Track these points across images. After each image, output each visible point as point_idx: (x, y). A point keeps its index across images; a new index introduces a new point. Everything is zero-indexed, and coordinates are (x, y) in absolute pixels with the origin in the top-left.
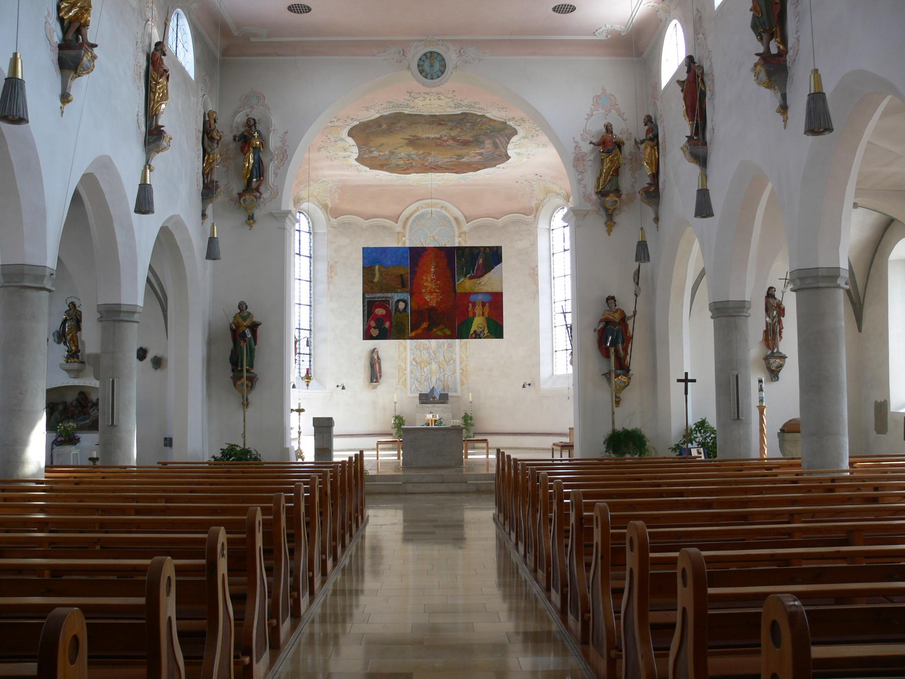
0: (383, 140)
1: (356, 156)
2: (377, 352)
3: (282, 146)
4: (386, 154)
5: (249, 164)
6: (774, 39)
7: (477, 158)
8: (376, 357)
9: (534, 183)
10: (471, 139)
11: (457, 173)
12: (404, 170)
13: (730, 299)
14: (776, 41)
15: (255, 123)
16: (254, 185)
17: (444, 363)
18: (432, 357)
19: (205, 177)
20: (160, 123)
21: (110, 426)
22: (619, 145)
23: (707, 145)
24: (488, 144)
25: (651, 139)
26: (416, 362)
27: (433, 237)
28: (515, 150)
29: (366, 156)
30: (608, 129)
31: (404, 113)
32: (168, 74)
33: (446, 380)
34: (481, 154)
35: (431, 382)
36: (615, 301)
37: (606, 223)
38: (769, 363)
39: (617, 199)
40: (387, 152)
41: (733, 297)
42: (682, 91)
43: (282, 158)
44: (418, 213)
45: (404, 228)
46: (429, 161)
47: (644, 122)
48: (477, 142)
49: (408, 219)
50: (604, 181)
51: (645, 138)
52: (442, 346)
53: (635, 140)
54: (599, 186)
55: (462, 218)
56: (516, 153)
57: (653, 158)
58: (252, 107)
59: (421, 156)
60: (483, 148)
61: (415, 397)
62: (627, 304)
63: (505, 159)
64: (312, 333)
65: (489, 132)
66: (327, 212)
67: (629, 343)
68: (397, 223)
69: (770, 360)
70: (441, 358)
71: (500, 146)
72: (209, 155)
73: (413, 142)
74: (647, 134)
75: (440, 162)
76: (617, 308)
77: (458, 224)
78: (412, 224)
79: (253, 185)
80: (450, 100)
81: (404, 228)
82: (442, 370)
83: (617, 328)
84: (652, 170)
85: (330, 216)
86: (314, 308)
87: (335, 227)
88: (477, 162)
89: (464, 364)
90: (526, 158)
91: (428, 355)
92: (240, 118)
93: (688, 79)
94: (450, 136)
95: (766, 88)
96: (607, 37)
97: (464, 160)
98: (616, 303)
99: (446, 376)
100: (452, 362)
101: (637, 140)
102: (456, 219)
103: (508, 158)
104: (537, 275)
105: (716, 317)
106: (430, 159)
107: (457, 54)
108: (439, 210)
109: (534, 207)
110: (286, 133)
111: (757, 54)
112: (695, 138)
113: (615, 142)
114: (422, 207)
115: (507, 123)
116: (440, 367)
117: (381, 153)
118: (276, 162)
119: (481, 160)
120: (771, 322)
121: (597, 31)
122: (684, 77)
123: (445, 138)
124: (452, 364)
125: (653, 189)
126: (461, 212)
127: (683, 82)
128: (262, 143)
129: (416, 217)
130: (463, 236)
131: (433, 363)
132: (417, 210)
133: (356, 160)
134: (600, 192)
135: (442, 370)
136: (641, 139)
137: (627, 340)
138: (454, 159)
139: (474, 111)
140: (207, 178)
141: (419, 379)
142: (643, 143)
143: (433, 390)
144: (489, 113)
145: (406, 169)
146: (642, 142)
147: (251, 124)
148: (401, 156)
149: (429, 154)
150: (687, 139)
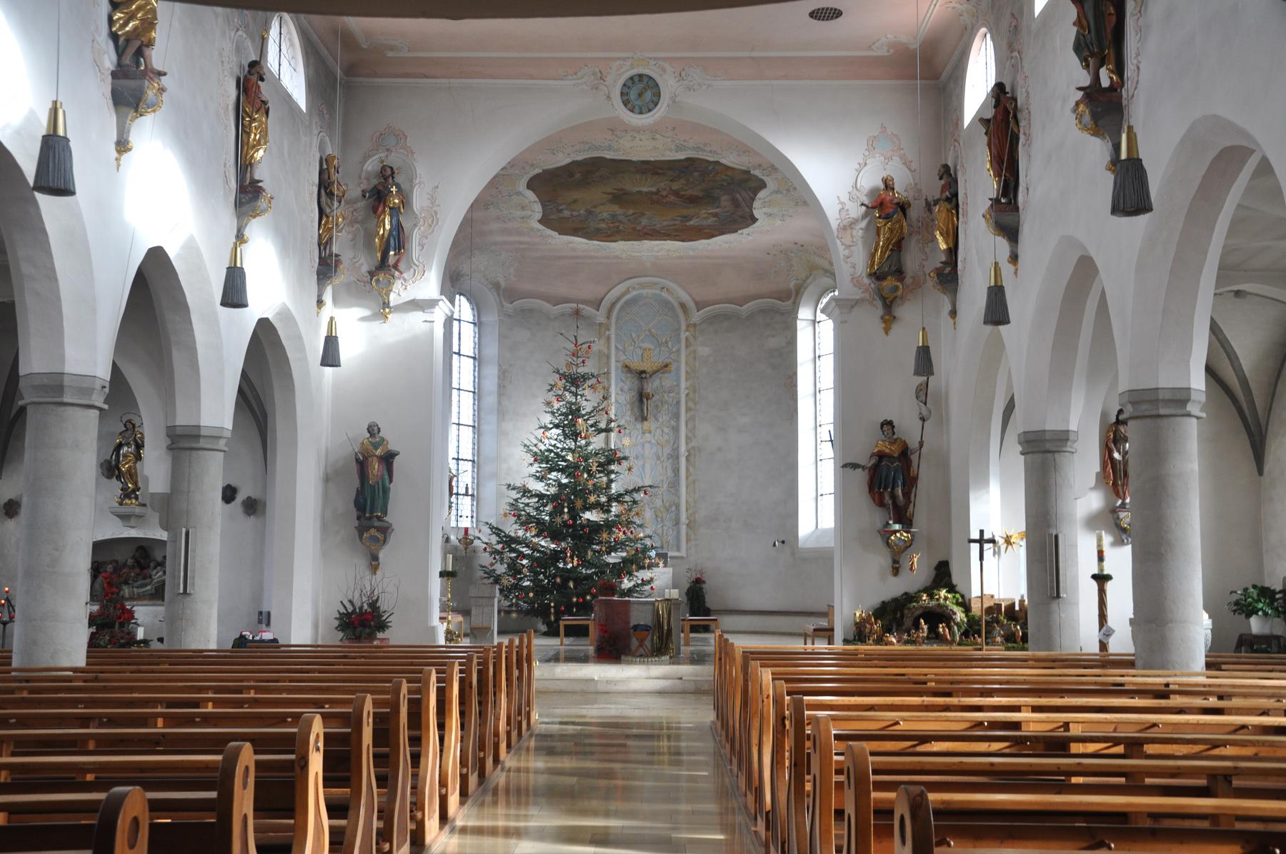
0: (576, 195)
1: (539, 216)
3: (431, 205)
4: (580, 214)
5: (384, 231)
6: (1105, 67)
7: (710, 220)
9: (792, 255)
10: (701, 194)
11: (683, 241)
12: (609, 236)
13: (1047, 428)
14: (1107, 69)
15: (393, 173)
16: (391, 261)
17: (662, 509)
19: (322, 248)
20: (257, 177)
21: (182, 594)
22: (903, 207)
23: (1018, 211)
24: (725, 200)
25: (948, 200)
27: (649, 331)
28: (764, 210)
29: (553, 217)
30: (888, 184)
31: (606, 159)
32: (267, 106)
33: (665, 532)
34: (715, 215)
36: (894, 427)
37: (882, 318)
38: (1118, 518)
39: (898, 284)
40: (582, 212)
41: (1051, 425)
42: (986, 134)
43: (430, 223)
45: (608, 317)
46: (642, 224)
47: (939, 174)
48: (708, 198)
49: (613, 305)
50: (881, 257)
51: (937, 196)
53: (926, 200)
54: (872, 266)
55: (691, 305)
56: (765, 213)
57: (950, 226)
58: (388, 150)
59: (632, 217)
60: (717, 207)
62: (909, 429)
63: (750, 221)
64: (476, 465)
65: (725, 184)
66: (499, 295)
67: (913, 487)
68: (598, 310)
69: (1120, 513)
71: (743, 204)
72: (328, 217)
73: (619, 198)
74: (943, 191)
75: (658, 226)
76: (895, 437)
77: (684, 312)
78: (620, 311)
79: (390, 261)
80: (669, 140)
82: (659, 519)
83: (895, 465)
84: (947, 243)
85: (503, 300)
87: (509, 316)
88: (709, 225)
89: (690, 511)
90: (781, 220)
92: (372, 165)
93: (995, 117)
94: (671, 189)
95: (1092, 135)
96: (888, 51)
97: (691, 223)
98: (895, 430)
99: (665, 528)
101: (929, 200)
102: (683, 306)
103: (754, 220)
105: (1027, 453)
106: (644, 221)
107: (676, 77)
108: (657, 292)
109: (793, 289)
110: (437, 187)
111: (1080, 89)
112: (1003, 201)
113: (898, 204)
114: (634, 288)
115: (752, 172)
116: (657, 516)
117: (574, 213)
118: (422, 228)
119: (716, 224)
120: (1121, 459)
121: (874, 44)
122: (989, 114)
123: (664, 193)
125: (948, 270)
126: (690, 295)
127: (989, 121)
128: (402, 202)
129: (625, 303)
132: (627, 292)
133: (540, 221)
134: (875, 273)
135: (659, 519)
136: (935, 198)
137: (911, 482)
138: (677, 222)
139: (706, 155)
140: (325, 249)
142: (937, 203)
144: (725, 158)
145: (611, 234)
146: (936, 202)
147: (387, 174)
148: (603, 217)
149: (643, 214)
150: (991, 202)
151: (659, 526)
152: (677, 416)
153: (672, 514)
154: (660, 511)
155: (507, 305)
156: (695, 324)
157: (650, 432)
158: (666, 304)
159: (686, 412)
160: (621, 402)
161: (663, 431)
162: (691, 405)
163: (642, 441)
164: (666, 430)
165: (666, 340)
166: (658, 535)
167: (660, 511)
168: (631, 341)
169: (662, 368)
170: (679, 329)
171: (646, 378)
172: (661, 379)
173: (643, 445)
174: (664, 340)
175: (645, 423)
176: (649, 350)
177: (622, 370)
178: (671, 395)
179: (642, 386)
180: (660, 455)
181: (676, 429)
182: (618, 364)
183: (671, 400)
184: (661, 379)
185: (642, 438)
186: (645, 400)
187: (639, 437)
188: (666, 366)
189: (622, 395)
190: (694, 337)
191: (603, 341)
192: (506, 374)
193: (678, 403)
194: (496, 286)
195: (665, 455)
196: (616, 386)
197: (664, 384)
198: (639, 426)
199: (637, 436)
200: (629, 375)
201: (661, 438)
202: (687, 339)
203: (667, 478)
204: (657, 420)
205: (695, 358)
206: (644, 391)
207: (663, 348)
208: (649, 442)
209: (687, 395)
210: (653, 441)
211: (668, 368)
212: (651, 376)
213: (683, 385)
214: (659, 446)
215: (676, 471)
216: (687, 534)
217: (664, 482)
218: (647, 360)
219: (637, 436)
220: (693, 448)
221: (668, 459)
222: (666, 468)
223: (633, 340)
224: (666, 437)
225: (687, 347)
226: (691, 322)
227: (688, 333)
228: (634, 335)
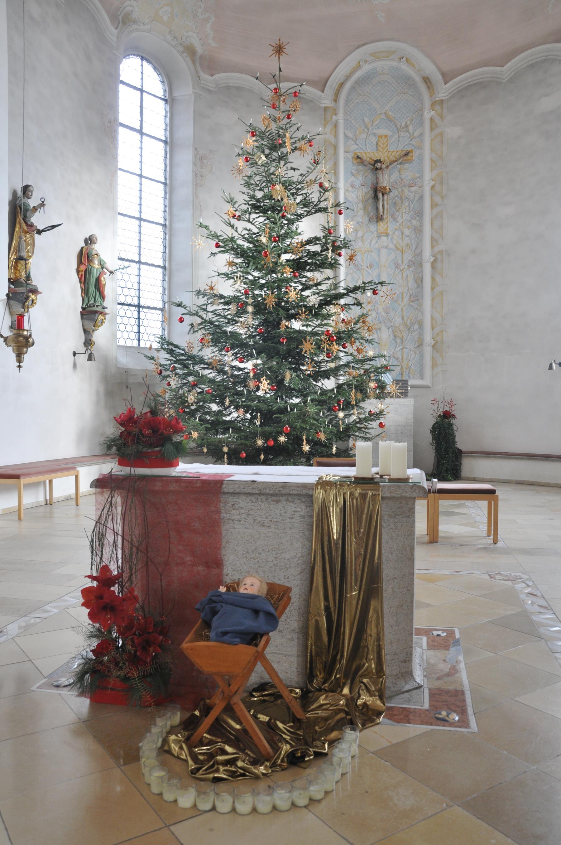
17: (402, 328)
18: (381, 319)
27: (385, 113)
33: (405, 357)
44: (359, 74)
45: (335, 101)
49: (342, 85)
52: (400, 299)
64: (167, 273)
66: (194, 62)
68: (323, 92)
70: (398, 321)
77: (428, 88)
78: (349, 93)
81: (335, 101)
82: (398, 340)
86: (171, 230)
87: (210, 91)
89: (437, 330)
102: (427, 80)
108: (395, 64)
114: (366, 61)
116: (395, 336)
124: (417, 330)
126: (435, 64)
130: (438, 107)
131: (384, 328)
132: (358, 67)
151: (398, 349)
152: (419, 214)
153: (414, 334)
154: (400, 331)
155: (205, 76)
156: (442, 100)
157: (387, 235)
158: (407, 80)
161: (402, 233)
162: (437, 199)
163: (377, 246)
164: (407, 232)
165: (407, 122)
167: (400, 331)
168: (363, 127)
169: (401, 158)
170: (422, 110)
171: (381, 169)
172: (399, 171)
173: (379, 251)
174: (403, 124)
175: (381, 223)
176: (386, 136)
177: (353, 163)
178: (413, 189)
179: (377, 178)
180: (400, 262)
181: (418, 230)
182: (348, 155)
183: (412, 195)
185: (377, 242)
186: (380, 195)
187: (374, 241)
188: (406, 155)
190: (442, 117)
191: (329, 128)
192: (205, 161)
193: (421, 198)
194: (191, 51)
195: (405, 262)
196: (346, 181)
197: (403, 176)
198: (373, 227)
199: (371, 241)
200: (361, 168)
201: (400, 242)
202: (432, 119)
204: (395, 219)
205: (442, 142)
206: (379, 186)
207: (402, 134)
208: (386, 247)
209: (433, 187)
210: (391, 246)
211: (409, 157)
212: (387, 167)
213: (427, 176)
214: (399, 252)
215: (419, 281)
216: (433, 358)
217: (405, 295)
218: (383, 149)
219: (371, 241)
220: (441, 252)
221: (409, 267)
222: (407, 277)
223: (366, 127)
224: (407, 240)
225: (432, 129)
226: (437, 99)
227: (433, 112)
228: (366, 120)
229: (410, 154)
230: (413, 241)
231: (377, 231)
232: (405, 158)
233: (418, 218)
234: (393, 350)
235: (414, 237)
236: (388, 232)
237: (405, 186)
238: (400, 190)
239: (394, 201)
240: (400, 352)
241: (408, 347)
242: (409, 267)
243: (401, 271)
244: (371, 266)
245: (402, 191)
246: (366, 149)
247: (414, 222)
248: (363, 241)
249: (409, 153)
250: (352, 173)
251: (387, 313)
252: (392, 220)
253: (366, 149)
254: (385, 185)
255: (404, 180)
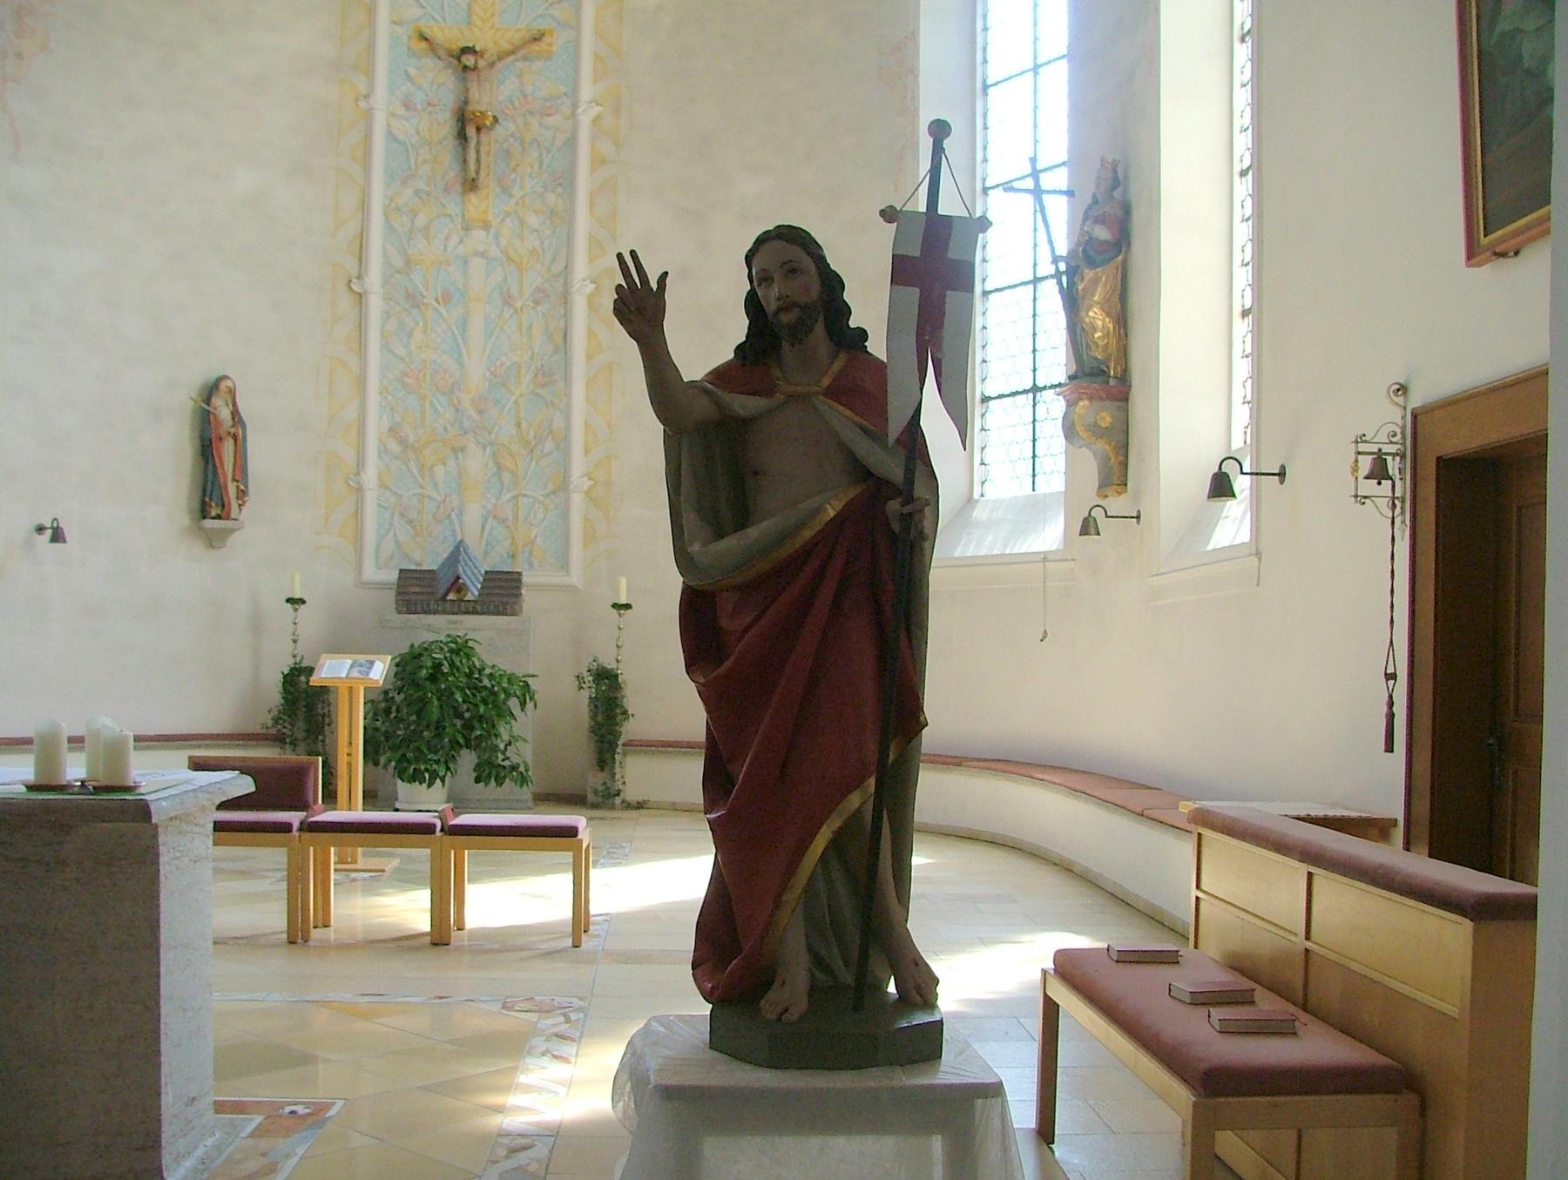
2: (232, 393)
8: (225, 413)
26: (403, 442)
33: (522, 515)
35: (461, 524)
61: (383, 586)
82: (506, 476)
91: (449, 414)
100: (549, 445)
104: (913, 72)
116: (499, 467)
124: (550, 453)
135: (506, 476)
141: (414, 515)
143: (457, 553)
152: (565, 181)
157: (486, 226)
159: (593, 171)
160: (401, 137)
163: (461, 250)
164: (533, 220)
166: (503, 521)
167: (511, 455)
171: (475, 68)
172: (520, 76)
173: (466, 262)
177: (409, 49)
178: (551, 121)
180: (515, 292)
181: (563, 219)
182: (399, 30)
184: (520, 76)
185: (461, 241)
186: (471, 131)
187: (455, 240)
188: (536, 39)
189: (407, 119)
193: (572, 142)
197: (529, 89)
198: (453, 208)
199: (447, 238)
200: (429, 62)
203: (532, 358)
204: (506, 190)
206: (470, 108)
208: (483, 255)
209: (596, 120)
212: (491, 65)
213: (587, 92)
221: (537, 303)
222: (530, 327)
229: (547, 39)
230: (546, 243)
231: (463, 216)
232: (535, 47)
233: (559, 190)
234: (493, 501)
235: (548, 232)
236: (490, 218)
237: (531, 113)
238: (520, 120)
239: (505, 146)
240: (511, 505)
241: (528, 493)
242: (537, 303)
243: (516, 312)
244: (446, 298)
245: (526, 124)
246: (444, 19)
247: (551, 199)
248: (427, 237)
249: (543, 35)
250: (407, 74)
251: (480, 412)
252: (498, 190)
253: (444, 19)
254: (483, 109)
255: (530, 99)
